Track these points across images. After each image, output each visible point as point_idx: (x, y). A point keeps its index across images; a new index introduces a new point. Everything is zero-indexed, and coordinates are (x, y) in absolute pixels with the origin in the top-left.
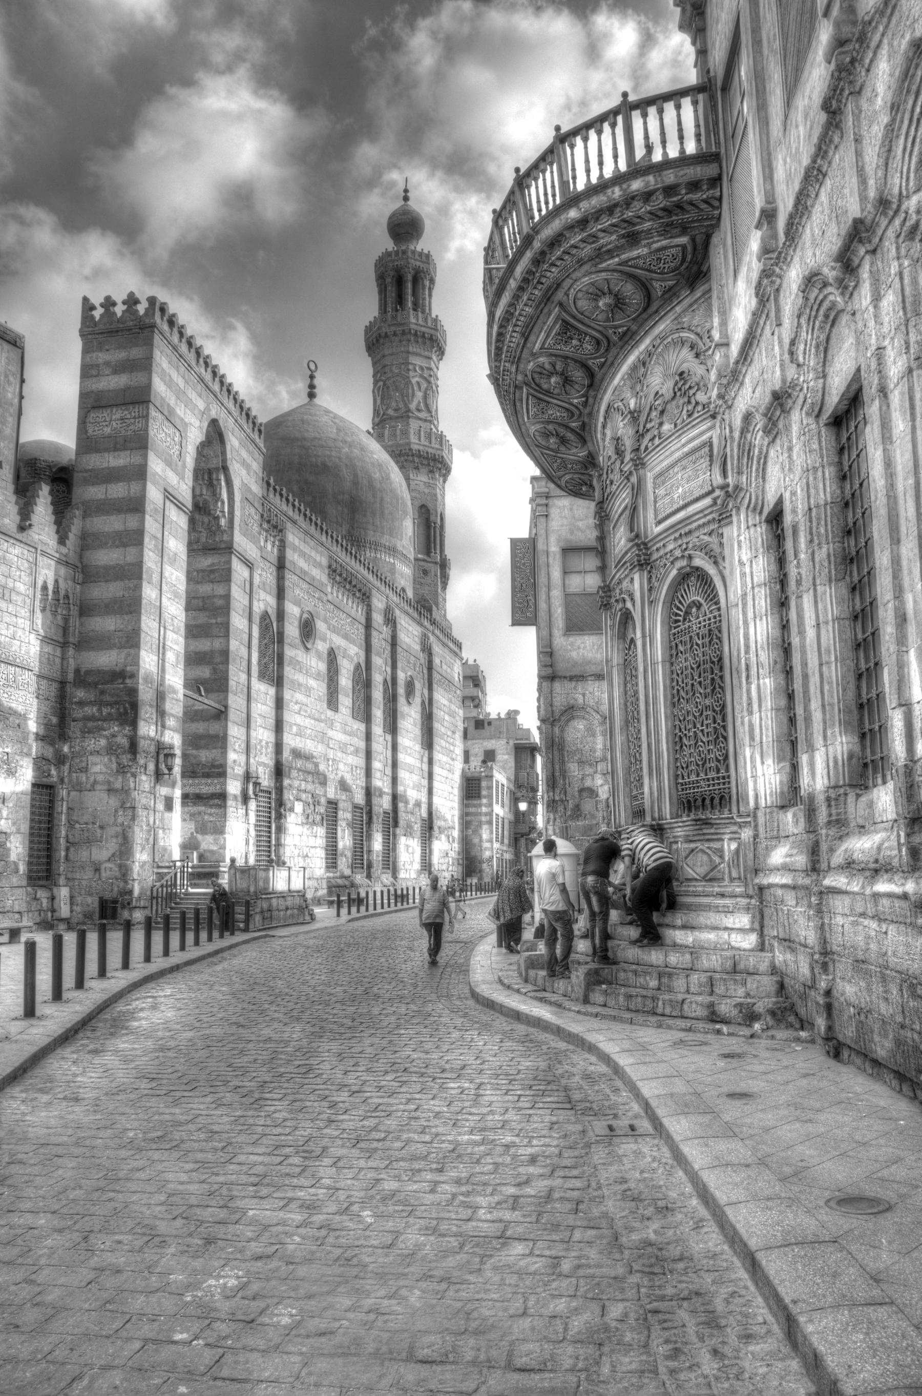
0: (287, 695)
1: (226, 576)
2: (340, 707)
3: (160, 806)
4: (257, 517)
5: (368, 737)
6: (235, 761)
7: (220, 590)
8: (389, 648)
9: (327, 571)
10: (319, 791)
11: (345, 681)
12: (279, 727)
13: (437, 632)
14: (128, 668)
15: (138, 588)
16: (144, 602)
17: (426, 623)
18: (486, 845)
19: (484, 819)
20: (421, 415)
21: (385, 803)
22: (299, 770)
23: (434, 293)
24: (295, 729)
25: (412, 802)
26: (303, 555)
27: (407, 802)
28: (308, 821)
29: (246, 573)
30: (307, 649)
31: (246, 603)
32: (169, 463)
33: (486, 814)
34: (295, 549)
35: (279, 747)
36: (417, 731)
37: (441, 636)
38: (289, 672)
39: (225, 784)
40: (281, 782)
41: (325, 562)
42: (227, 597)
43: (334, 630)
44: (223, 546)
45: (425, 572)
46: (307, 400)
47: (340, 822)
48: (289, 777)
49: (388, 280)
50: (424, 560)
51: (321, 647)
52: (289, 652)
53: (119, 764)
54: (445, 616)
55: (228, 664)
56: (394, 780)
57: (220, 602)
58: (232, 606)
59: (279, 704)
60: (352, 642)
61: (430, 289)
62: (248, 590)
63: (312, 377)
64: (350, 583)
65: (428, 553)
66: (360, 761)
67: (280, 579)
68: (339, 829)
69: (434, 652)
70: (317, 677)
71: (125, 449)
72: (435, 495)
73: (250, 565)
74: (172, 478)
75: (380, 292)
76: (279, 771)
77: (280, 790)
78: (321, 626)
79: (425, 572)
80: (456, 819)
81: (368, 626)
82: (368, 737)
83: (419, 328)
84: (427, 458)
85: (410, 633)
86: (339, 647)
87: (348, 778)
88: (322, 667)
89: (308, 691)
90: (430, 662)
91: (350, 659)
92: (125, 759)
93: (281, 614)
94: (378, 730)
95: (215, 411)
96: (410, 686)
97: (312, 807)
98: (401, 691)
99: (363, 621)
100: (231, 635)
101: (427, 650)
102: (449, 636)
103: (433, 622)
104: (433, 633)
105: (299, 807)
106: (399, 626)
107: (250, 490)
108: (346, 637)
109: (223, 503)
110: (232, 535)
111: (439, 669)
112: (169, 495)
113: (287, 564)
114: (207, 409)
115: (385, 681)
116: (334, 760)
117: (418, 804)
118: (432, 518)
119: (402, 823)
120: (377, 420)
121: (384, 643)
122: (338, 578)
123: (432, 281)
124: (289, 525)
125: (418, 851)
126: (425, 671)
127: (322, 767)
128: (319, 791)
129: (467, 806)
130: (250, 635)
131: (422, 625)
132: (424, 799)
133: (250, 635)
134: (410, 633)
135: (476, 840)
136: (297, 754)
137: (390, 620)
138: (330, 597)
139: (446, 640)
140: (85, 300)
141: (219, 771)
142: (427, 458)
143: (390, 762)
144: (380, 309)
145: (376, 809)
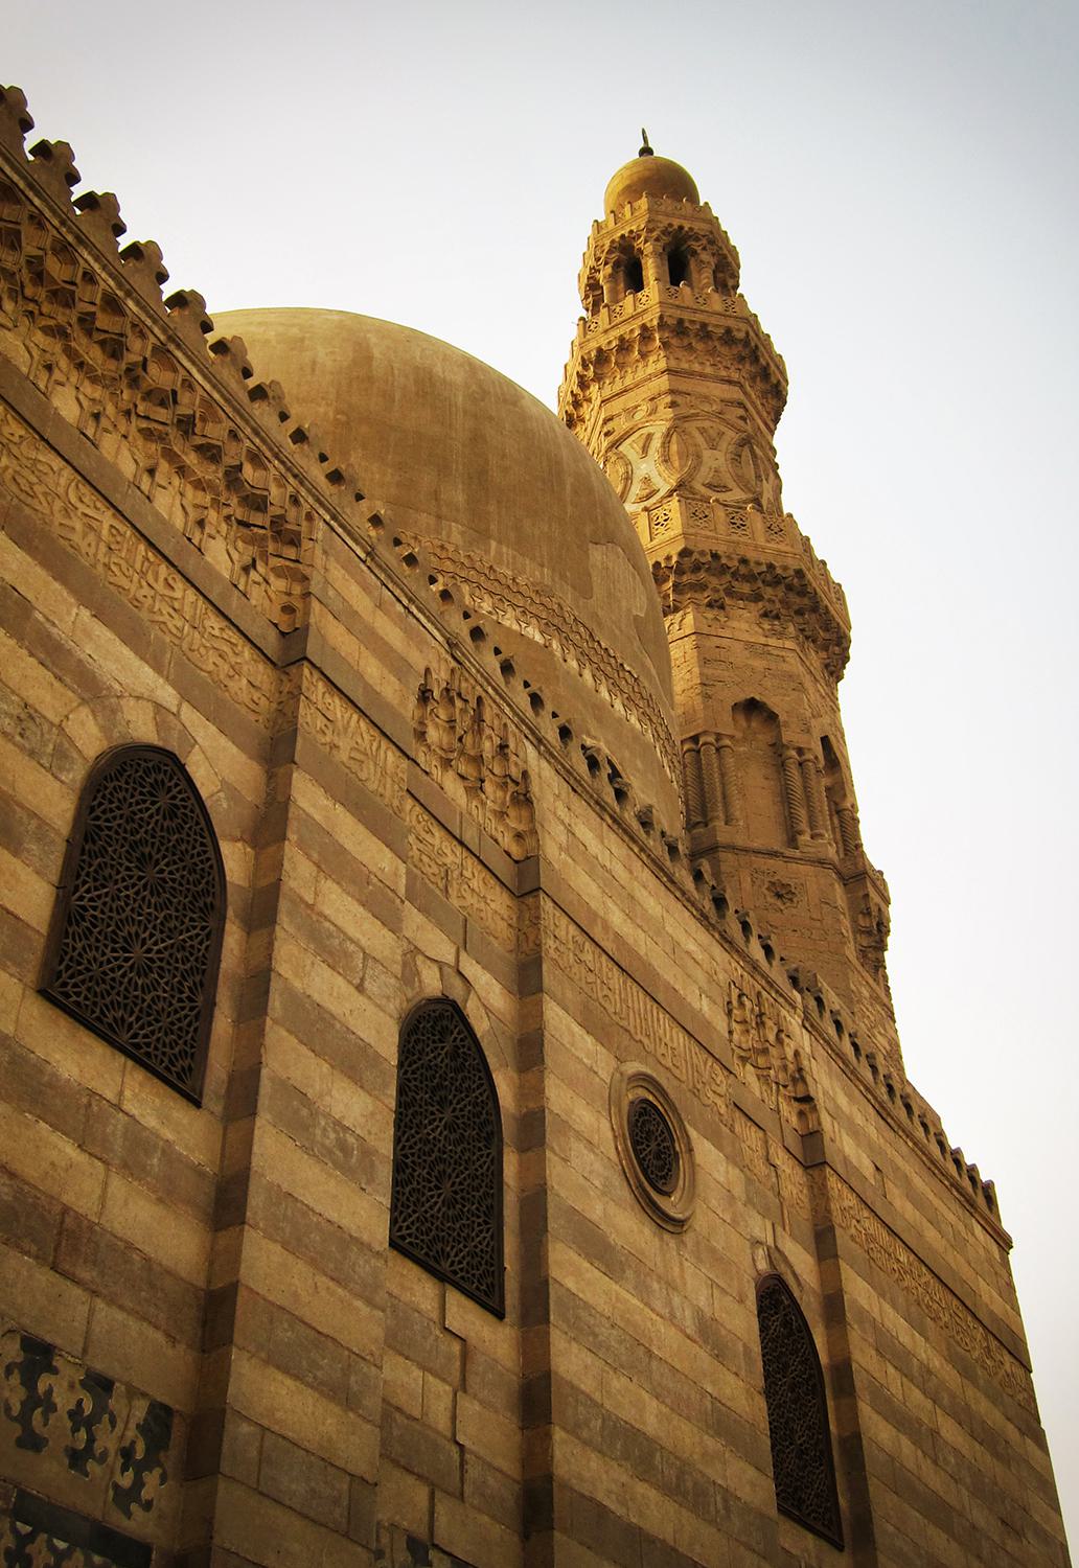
45: (782, 892)
65: (792, 841)
83: (686, 316)
84: (750, 578)
118: (787, 736)
142: (750, 578)
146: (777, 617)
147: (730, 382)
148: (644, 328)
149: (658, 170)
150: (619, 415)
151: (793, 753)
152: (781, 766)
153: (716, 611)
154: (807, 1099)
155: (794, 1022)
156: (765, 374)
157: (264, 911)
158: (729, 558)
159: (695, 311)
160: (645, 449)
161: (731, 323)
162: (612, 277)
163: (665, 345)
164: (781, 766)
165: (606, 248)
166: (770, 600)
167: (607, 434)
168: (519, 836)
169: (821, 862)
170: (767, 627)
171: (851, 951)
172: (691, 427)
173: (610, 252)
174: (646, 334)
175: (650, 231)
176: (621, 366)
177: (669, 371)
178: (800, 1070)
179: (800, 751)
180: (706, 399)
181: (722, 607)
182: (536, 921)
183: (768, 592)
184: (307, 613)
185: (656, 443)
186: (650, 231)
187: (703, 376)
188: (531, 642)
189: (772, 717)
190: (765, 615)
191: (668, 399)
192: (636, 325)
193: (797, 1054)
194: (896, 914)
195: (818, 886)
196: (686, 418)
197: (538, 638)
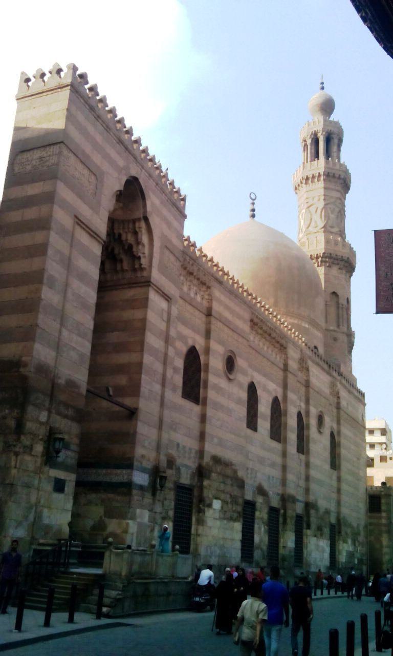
0: (210, 412)
1: (144, 303)
2: (259, 428)
3: (49, 487)
4: (178, 264)
5: (284, 454)
6: (143, 456)
7: (138, 314)
8: (303, 389)
9: (249, 323)
10: (236, 492)
11: (264, 408)
12: (202, 436)
13: (344, 382)
14: (24, 359)
15: (39, 291)
16: (43, 303)
17: (335, 374)
18: (385, 550)
19: (384, 528)
21: (299, 508)
22: (219, 474)
23: (342, 148)
24: (216, 440)
25: (322, 511)
26: (227, 308)
27: (317, 509)
28: (226, 516)
29: (164, 305)
30: (230, 380)
32: (81, 196)
33: (385, 525)
34: (220, 302)
35: (201, 453)
36: (327, 454)
37: (347, 385)
38: (211, 394)
39: (130, 475)
40: (202, 482)
41: (247, 316)
42: (144, 320)
44: (143, 280)
45: (335, 339)
46: (249, 219)
47: (256, 521)
48: (209, 478)
49: (309, 141)
51: (245, 381)
52: (212, 379)
53: (5, 443)
54: (351, 372)
55: (141, 374)
56: (307, 490)
58: (147, 328)
59: (203, 419)
60: (273, 381)
61: (339, 146)
62: (165, 318)
63: (253, 204)
64: (270, 335)
66: (276, 473)
68: (256, 526)
69: (340, 395)
70: (239, 402)
71: (40, 181)
73: (167, 298)
74: (86, 212)
75: (304, 150)
76: (201, 473)
77: (201, 488)
78: (240, 362)
80: (361, 528)
82: (284, 454)
83: (330, 171)
84: (337, 259)
87: (266, 486)
88: (244, 395)
89: (229, 412)
90: (338, 404)
91: (268, 392)
92: (11, 438)
93: (207, 351)
94: (292, 448)
95: (134, 171)
96: (320, 419)
97: (230, 506)
98: (313, 422)
99: (282, 366)
104: (341, 383)
105: (217, 504)
106: (311, 373)
107: (170, 241)
108: (265, 375)
109: (143, 245)
110: (151, 272)
112: (79, 222)
113: (213, 313)
115: (299, 414)
116: (252, 469)
117: (327, 512)
119: (313, 526)
121: (299, 385)
122: (260, 331)
123: (340, 141)
125: (328, 550)
126: (335, 410)
127: (240, 474)
128: (236, 492)
129: (370, 517)
131: (331, 375)
132: (333, 507)
134: (319, 379)
135: (378, 546)
136: (216, 460)
139: (351, 389)
140: (23, 73)
141: (128, 464)
143: (303, 476)
145: (290, 513)
147: (338, 191)
148: (319, 173)
152: (338, 308)
154: (339, 397)
155: (338, 384)
156: (347, 185)
157: (286, 415)
159: (333, 169)
160: (316, 211)
161: (341, 173)
162: (311, 143)
163: (324, 180)
165: (310, 134)
166: (341, 265)
167: (307, 203)
168: (307, 376)
169: (343, 333)
171: (346, 353)
172: (329, 206)
173: (312, 134)
174: (319, 175)
176: (312, 182)
180: (332, 197)
184: (287, 361)
185: (319, 211)
186: (323, 132)
187: (332, 190)
190: (339, 269)
194: (357, 341)
195: (343, 338)
197: (307, 326)
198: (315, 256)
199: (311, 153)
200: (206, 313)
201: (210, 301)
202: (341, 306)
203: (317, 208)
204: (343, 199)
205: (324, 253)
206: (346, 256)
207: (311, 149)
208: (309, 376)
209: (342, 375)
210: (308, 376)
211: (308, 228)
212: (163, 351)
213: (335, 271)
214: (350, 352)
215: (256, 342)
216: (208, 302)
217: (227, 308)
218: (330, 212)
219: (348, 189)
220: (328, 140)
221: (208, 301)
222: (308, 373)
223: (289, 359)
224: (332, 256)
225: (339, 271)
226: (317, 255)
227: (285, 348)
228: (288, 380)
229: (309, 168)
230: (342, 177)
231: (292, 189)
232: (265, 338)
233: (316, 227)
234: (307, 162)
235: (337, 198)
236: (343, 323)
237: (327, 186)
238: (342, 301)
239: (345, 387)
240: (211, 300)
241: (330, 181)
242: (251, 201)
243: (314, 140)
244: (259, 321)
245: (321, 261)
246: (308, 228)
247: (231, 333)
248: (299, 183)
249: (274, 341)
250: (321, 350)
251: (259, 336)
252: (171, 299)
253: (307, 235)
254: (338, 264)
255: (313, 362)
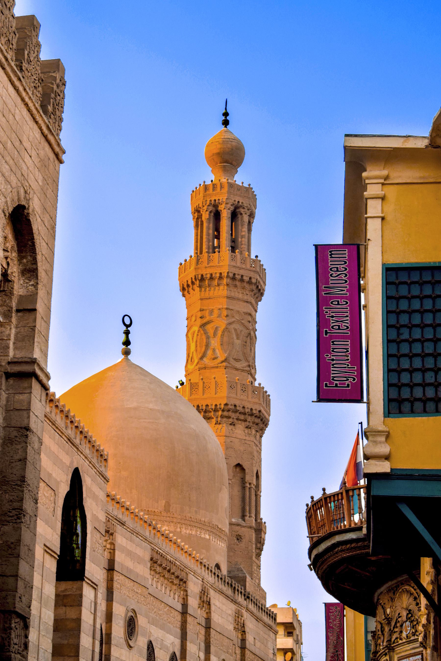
8: (203, 631)
13: (251, 607)
17: (240, 599)
20: (238, 365)
26: (130, 554)
30: (130, 647)
31: (91, 622)
42: (78, 621)
43: (153, 622)
45: (239, 538)
46: (121, 358)
49: (205, 216)
50: (238, 525)
54: (259, 584)
57: (71, 625)
58: (81, 630)
61: (250, 224)
62: (93, 612)
63: (127, 333)
64: (169, 571)
65: (243, 517)
67: (110, 581)
69: (247, 629)
72: (251, 453)
73: (94, 586)
75: (197, 226)
78: (141, 621)
79: (239, 538)
81: (184, 612)
83: (236, 271)
84: (244, 414)
85: (223, 612)
86: (156, 639)
90: (243, 640)
100: (80, 655)
101: (241, 629)
102: (262, 608)
103: (247, 597)
104: (247, 610)
106: (213, 608)
108: (162, 628)
109: (77, 535)
111: (252, 648)
113: (116, 568)
114: (72, 462)
118: (248, 478)
120: (191, 367)
121: (199, 627)
122: (159, 569)
123: (252, 215)
124: (119, 528)
126: (238, 651)
130: (93, 651)
131: (234, 602)
133: (93, 651)
134: (223, 612)
137: (205, 603)
138: (150, 591)
142: (244, 414)
144: (196, 248)
146: (250, 428)
148: (221, 274)
149: (232, 149)
150: (206, 310)
151: (248, 485)
152: (244, 488)
153: (232, 426)
154: (244, 632)
155: (244, 611)
158: (239, 406)
159: (240, 268)
162: (209, 219)
164: (244, 488)
165: (208, 203)
168: (207, 613)
169: (251, 527)
170: (246, 432)
171: (254, 558)
172: (232, 326)
175: (227, 204)
177: (228, 297)
178: (244, 624)
179: (250, 484)
181: (234, 425)
182: (209, 635)
183: (249, 419)
185: (219, 333)
187: (239, 299)
188: (207, 539)
189: (243, 469)
191: (225, 313)
192: (218, 271)
193: (244, 620)
196: (230, 324)
197: (207, 537)
198: (213, 407)
199: (208, 234)
200: (107, 569)
201: (112, 551)
202: (248, 485)
203: (217, 328)
204: (253, 313)
205: (226, 405)
206: (256, 408)
207: (208, 228)
208: (210, 612)
209: (248, 597)
210: (209, 613)
211: (201, 358)
212: (91, 648)
213: (240, 430)
214: (259, 555)
215: (154, 586)
216: (110, 552)
217: (130, 554)
218: (235, 338)
219: (262, 294)
220: (234, 216)
221: (109, 550)
222: (210, 609)
223: (189, 598)
224: (238, 408)
225: (246, 431)
226: (216, 405)
227: (185, 582)
228: (188, 625)
229: (205, 264)
230: (254, 281)
231: (177, 287)
232: (164, 576)
233: (214, 359)
234: (201, 253)
235: (246, 313)
236: (250, 513)
237: (233, 294)
238: (250, 478)
239: (252, 613)
240: (114, 550)
241: (236, 286)
242: (125, 328)
243: (212, 214)
244: (159, 557)
245: (222, 417)
246: (201, 358)
247: (132, 584)
248: (190, 283)
249: (173, 577)
250: (224, 570)
251: (157, 576)
252: (97, 586)
253: (200, 369)
254: (245, 421)
255: (215, 590)
